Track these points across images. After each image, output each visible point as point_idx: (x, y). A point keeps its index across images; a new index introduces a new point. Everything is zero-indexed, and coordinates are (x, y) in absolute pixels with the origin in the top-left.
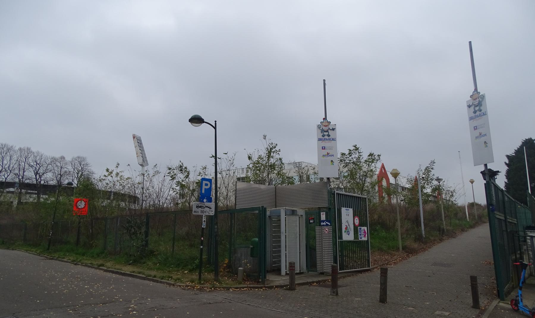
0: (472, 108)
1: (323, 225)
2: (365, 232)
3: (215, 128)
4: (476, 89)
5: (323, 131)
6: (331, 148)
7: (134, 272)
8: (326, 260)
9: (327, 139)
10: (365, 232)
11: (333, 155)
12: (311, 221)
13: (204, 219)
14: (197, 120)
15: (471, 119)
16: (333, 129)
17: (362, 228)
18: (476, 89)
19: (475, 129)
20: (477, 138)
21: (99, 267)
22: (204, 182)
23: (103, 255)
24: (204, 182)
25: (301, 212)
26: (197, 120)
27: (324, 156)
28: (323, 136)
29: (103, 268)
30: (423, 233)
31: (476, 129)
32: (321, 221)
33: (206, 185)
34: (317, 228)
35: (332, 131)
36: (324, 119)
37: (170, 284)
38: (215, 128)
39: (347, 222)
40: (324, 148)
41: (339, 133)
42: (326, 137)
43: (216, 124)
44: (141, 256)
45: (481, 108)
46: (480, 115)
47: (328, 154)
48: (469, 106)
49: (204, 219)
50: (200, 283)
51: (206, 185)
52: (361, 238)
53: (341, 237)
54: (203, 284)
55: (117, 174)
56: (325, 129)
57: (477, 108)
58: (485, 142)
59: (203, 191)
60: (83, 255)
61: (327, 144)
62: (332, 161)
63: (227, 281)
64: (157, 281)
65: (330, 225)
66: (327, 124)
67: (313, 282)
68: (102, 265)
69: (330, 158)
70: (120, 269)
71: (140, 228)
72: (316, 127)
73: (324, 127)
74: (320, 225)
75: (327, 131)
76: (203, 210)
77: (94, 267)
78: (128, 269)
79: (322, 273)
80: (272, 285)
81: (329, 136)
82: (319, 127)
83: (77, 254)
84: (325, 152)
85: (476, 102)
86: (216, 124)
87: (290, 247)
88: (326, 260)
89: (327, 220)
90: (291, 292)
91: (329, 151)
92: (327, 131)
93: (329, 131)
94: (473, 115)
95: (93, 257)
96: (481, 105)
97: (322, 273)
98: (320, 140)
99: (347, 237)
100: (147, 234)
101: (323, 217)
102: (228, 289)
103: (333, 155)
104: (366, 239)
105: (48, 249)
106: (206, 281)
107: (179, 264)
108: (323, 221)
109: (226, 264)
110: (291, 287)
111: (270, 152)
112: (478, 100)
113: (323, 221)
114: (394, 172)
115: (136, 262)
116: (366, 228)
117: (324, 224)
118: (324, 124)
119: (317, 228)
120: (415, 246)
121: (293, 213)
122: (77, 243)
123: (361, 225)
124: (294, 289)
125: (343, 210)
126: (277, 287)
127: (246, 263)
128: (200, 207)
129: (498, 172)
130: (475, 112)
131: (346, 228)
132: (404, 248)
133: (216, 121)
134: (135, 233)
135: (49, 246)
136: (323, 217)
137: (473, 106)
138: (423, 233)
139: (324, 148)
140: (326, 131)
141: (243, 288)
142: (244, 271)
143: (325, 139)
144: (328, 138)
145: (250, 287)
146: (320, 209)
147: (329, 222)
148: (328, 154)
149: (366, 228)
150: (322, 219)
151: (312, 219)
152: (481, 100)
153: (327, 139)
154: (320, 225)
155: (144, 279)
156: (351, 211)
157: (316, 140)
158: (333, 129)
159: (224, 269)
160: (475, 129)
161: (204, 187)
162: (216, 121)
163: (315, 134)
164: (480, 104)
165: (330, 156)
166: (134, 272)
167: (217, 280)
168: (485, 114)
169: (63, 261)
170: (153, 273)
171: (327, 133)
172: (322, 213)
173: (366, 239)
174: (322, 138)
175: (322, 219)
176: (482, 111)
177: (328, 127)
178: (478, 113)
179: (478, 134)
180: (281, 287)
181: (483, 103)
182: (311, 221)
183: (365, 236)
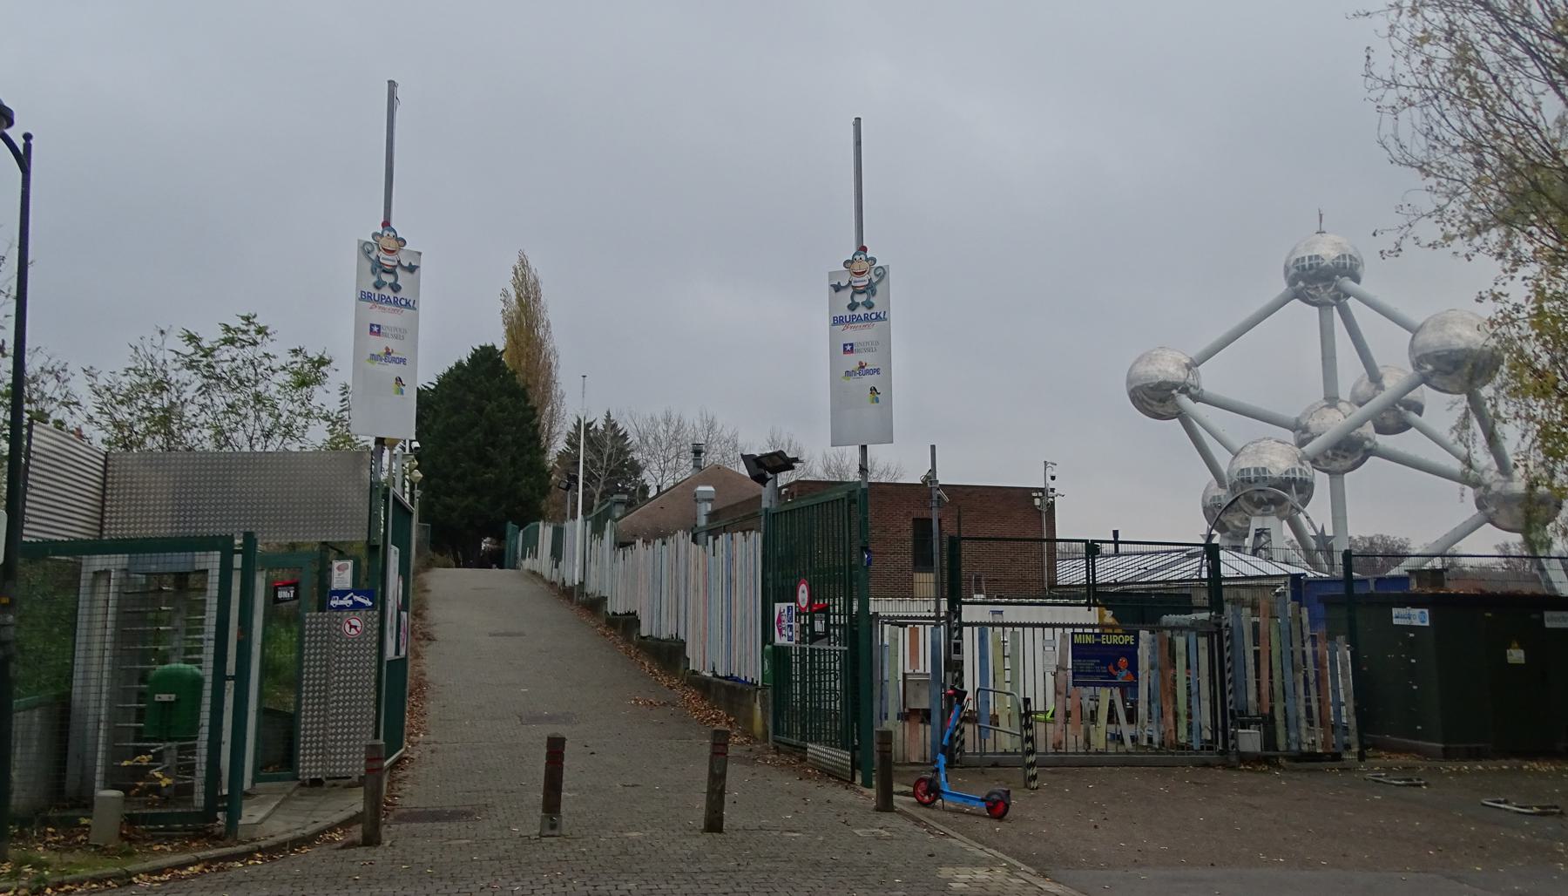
0: (845, 297)
5: (378, 267)
9: (388, 301)
11: (403, 361)
16: (412, 269)
27: (374, 357)
28: (378, 286)
31: (852, 351)
32: (325, 592)
34: (311, 616)
40: (376, 330)
41: (429, 287)
42: (387, 292)
45: (873, 300)
46: (867, 318)
56: (388, 261)
57: (860, 299)
58: (873, 390)
61: (387, 317)
62: (399, 380)
65: (373, 608)
66: (392, 245)
69: (393, 370)
73: (382, 255)
74: (323, 606)
75: (392, 272)
81: (396, 288)
84: (377, 345)
85: (862, 282)
91: (392, 343)
93: (398, 270)
96: (874, 294)
101: (342, 576)
103: (403, 361)
112: (866, 277)
113: (342, 594)
117: (346, 602)
118: (384, 242)
119: (311, 616)
130: (853, 306)
136: (342, 576)
137: (850, 291)
139: (376, 330)
140: (388, 270)
143: (382, 297)
144: (392, 295)
146: (330, 551)
147: (369, 594)
148: (388, 353)
151: (286, 585)
152: (875, 280)
153: (388, 301)
154: (323, 606)
164: (870, 289)
165: (394, 360)
171: (389, 279)
172: (336, 564)
174: (373, 291)
176: (874, 310)
178: (861, 311)
179: (854, 366)
181: (879, 288)
182: (282, 594)
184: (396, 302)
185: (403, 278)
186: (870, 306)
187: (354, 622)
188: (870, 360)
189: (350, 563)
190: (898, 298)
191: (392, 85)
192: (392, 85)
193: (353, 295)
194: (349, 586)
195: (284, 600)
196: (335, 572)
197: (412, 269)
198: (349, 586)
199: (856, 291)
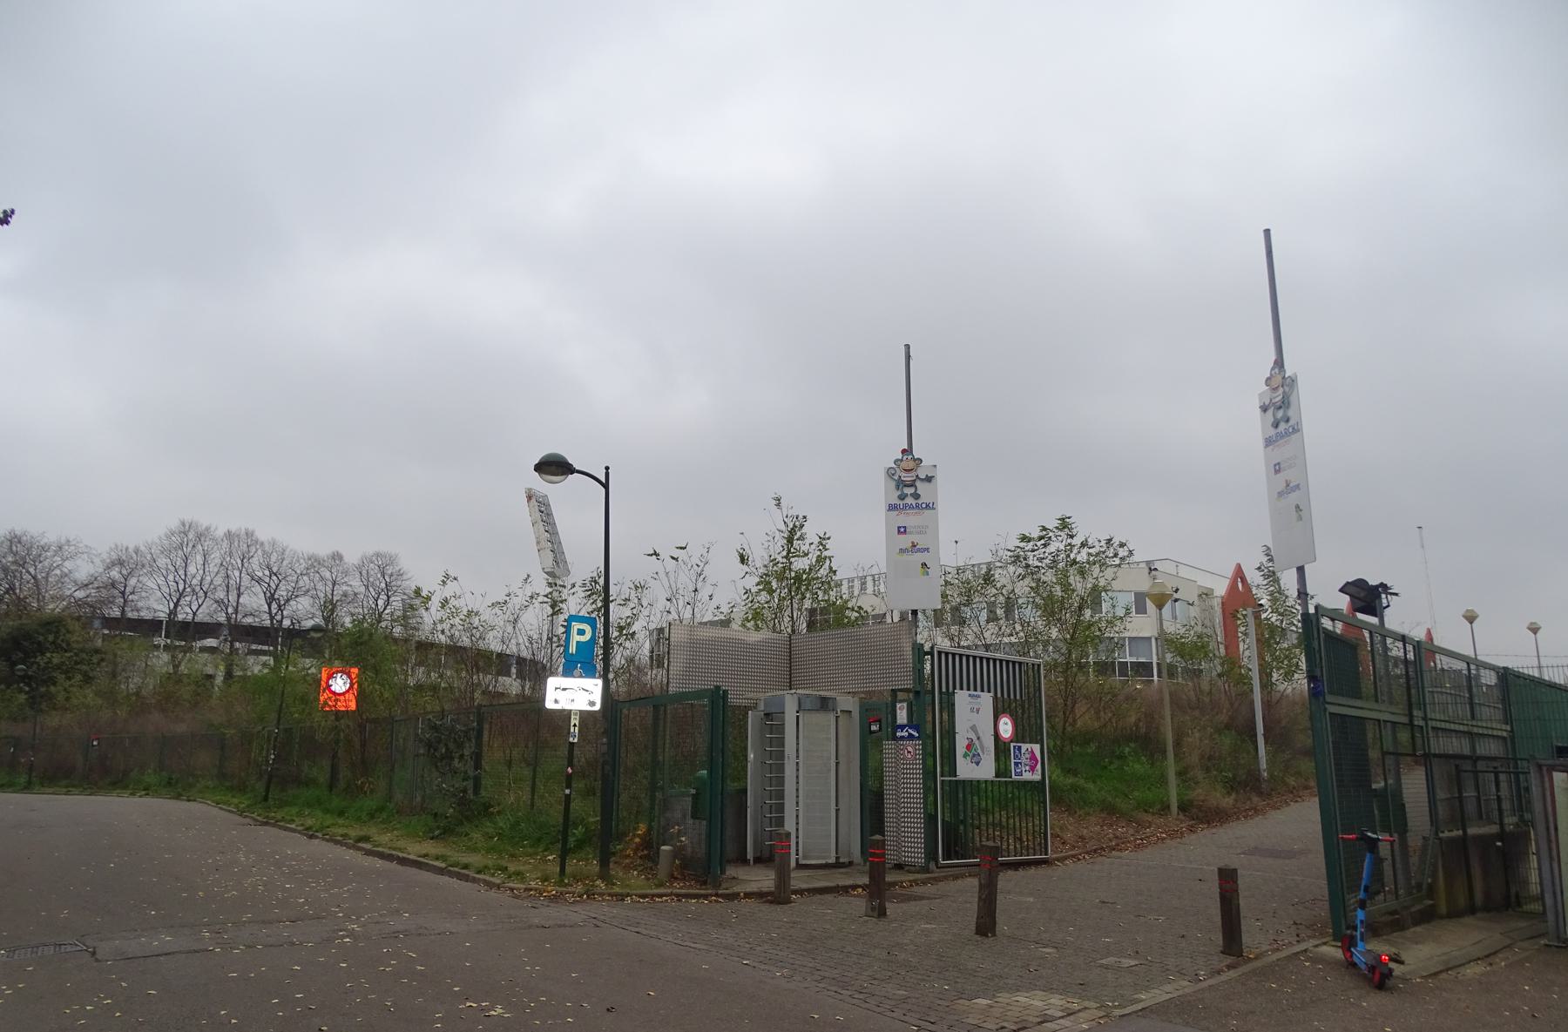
2: (1033, 757)
3: (606, 486)
4: (1279, 363)
5: (901, 484)
6: (922, 531)
7: (425, 856)
8: (907, 835)
9: (911, 507)
11: (927, 550)
12: (875, 724)
13: (575, 720)
15: (1269, 442)
16: (929, 479)
17: (1024, 747)
18: (1279, 363)
19: (1277, 472)
20: (1280, 494)
22: (576, 626)
23: (384, 815)
24: (576, 626)
25: (847, 703)
27: (902, 551)
28: (902, 497)
29: (368, 846)
30: (1263, 765)
34: (888, 745)
35: (926, 484)
36: (904, 451)
37: (490, 885)
38: (606, 486)
39: (974, 728)
40: (902, 531)
42: (910, 500)
44: (462, 814)
45: (1290, 413)
48: (1264, 409)
49: (575, 720)
50: (560, 883)
51: (581, 632)
54: (566, 885)
55: (444, 603)
56: (907, 477)
57: (1280, 414)
58: (1297, 507)
59: (573, 649)
60: (341, 814)
61: (911, 520)
62: (924, 565)
63: (636, 880)
64: (466, 878)
66: (911, 465)
67: (854, 887)
68: (366, 839)
69: (919, 558)
70: (400, 850)
71: (460, 746)
72: (882, 475)
75: (912, 484)
77: (345, 845)
78: (414, 849)
80: (736, 889)
81: (916, 496)
82: (890, 473)
83: (326, 811)
87: (811, 794)
89: (910, 725)
90: (779, 908)
92: (912, 484)
93: (918, 484)
94: (1272, 432)
95: (359, 819)
98: (892, 508)
99: (976, 769)
100: (477, 759)
101: (902, 716)
103: (927, 550)
104: (1037, 777)
105: (266, 799)
106: (577, 878)
107: (539, 840)
108: (902, 727)
110: (779, 896)
111: (790, 540)
113: (902, 727)
115: (445, 831)
117: (905, 734)
118: (904, 465)
119: (888, 745)
120: (1222, 799)
121: (825, 704)
123: (1020, 735)
124: (788, 901)
125: (962, 698)
126: (748, 895)
127: (689, 835)
129: (1341, 590)
130: (1276, 425)
131: (968, 747)
132: (1184, 808)
134: (449, 756)
135: (267, 791)
136: (902, 716)
138: (1263, 765)
139: (902, 531)
140: (909, 483)
141: (660, 896)
142: (678, 853)
143: (905, 506)
145: (677, 895)
147: (917, 728)
149: (1036, 748)
150: (899, 721)
153: (911, 507)
154: (895, 738)
155: (441, 871)
156: (986, 700)
157: (883, 508)
158: (929, 479)
160: (1277, 472)
161: (576, 638)
163: (880, 492)
164: (1285, 404)
165: (919, 550)
166: (425, 856)
167: (604, 875)
168: (1296, 430)
169: (286, 829)
170: (475, 859)
175: (899, 721)
177: (913, 473)
178: (1283, 426)
179: (1282, 486)
180: (760, 895)
181: (1293, 399)
182: (874, 728)
183: (1033, 769)
190: (1309, 407)
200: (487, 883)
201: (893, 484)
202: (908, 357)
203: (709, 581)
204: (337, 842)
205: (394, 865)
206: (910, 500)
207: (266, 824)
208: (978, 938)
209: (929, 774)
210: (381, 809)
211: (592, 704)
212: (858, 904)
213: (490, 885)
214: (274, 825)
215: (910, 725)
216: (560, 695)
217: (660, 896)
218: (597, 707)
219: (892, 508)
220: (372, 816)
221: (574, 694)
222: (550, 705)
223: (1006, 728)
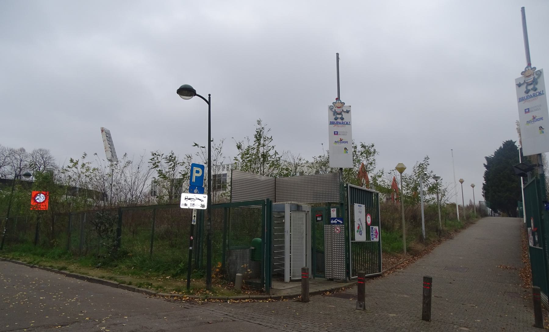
0: (523, 88)
1: (334, 224)
2: (376, 232)
3: (209, 103)
4: (529, 64)
5: (335, 113)
6: (345, 134)
7: (103, 277)
8: (336, 265)
9: (340, 123)
10: (376, 232)
12: (319, 217)
13: (194, 214)
14: (186, 91)
15: (521, 100)
16: (348, 112)
17: (374, 227)
18: (529, 64)
20: (528, 122)
21: (60, 270)
22: (195, 169)
23: (66, 256)
24: (195, 169)
25: (306, 207)
26: (186, 91)
29: (65, 272)
30: (424, 234)
32: (330, 219)
33: (197, 172)
34: (327, 227)
35: (346, 114)
36: (337, 99)
37: (150, 294)
38: (209, 103)
39: (360, 220)
40: (336, 133)
42: (339, 120)
43: (210, 98)
44: (113, 257)
45: (537, 86)
46: (535, 95)
47: (341, 140)
48: (519, 85)
49: (194, 214)
50: (188, 293)
52: (373, 239)
53: (353, 239)
54: (192, 294)
56: (338, 110)
57: (530, 87)
59: (194, 180)
60: (42, 255)
61: (339, 129)
62: (346, 149)
63: (223, 290)
64: (134, 290)
66: (340, 105)
67: (326, 291)
68: (65, 268)
69: (344, 145)
70: (86, 274)
71: (111, 225)
73: (336, 109)
76: (193, 202)
77: (54, 271)
78: (95, 273)
79: (331, 280)
81: (342, 119)
82: (331, 108)
83: (34, 254)
84: (337, 138)
85: (531, 79)
86: (210, 98)
88: (336, 265)
89: (338, 218)
90: (306, 304)
91: (342, 137)
93: (343, 113)
94: (525, 95)
95: (53, 258)
96: (537, 83)
97: (331, 280)
98: (331, 123)
99: (360, 237)
100: (119, 232)
101: (334, 214)
102: (225, 300)
106: (197, 290)
107: (159, 268)
108: (334, 219)
109: (218, 268)
110: (304, 298)
112: (532, 77)
113: (334, 219)
114: (400, 167)
115: (105, 265)
116: (377, 228)
117: (335, 222)
118: (337, 105)
119: (327, 227)
120: (420, 247)
121: (298, 208)
122: (36, 242)
123: (374, 223)
124: (308, 301)
126: (285, 297)
127: (242, 268)
128: (189, 199)
130: (527, 92)
131: (359, 228)
132: (409, 250)
133: (210, 95)
134: (106, 230)
136: (334, 214)
137: (525, 85)
138: (424, 234)
139: (336, 133)
141: (244, 299)
142: (243, 277)
143: (337, 122)
144: (341, 121)
145: (253, 299)
146: (329, 205)
148: (341, 140)
149: (377, 228)
150: (332, 216)
152: (536, 77)
153: (340, 123)
154: (330, 223)
156: (363, 206)
159: (216, 275)
160: (526, 112)
161: (195, 175)
162: (210, 95)
163: (325, 116)
164: (535, 82)
165: (343, 142)
166: (103, 277)
168: (542, 93)
169: (16, 263)
170: (127, 279)
171: (339, 116)
172: (332, 209)
173: (378, 240)
174: (334, 121)
175: (332, 216)
176: (537, 91)
177: (341, 109)
178: (531, 93)
179: (531, 118)
180: (290, 297)
181: (539, 80)
182: (318, 219)
184: (343, 123)
185: (345, 115)
186: (535, 89)
187: (338, 228)
188: (538, 115)
189: (335, 209)
191: (338, 54)
192: (338, 54)
193: (327, 122)
194: (335, 216)
195: (319, 221)
196: (332, 212)
197: (348, 112)
198: (335, 216)
199: (529, 84)
200: (147, 293)
201: (332, 113)
202: (338, 59)
203: (223, 155)
204: (48, 270)
205: (86, 283)
206: (339, 120)
207: (5, 260)
208: (424, 322)
209: (347, 239)
210: (64, 253)
211: (203, 206)
212: (352, 303)
213: (150, 294)
214: (9, 261)
215: (338, 218)
216: (189, 202)
217: (244, 299)
218: (205, 208)
219: (331, 123)
220: (60, 257)
221: (194, 202)
222: (182, 206)
223: (369, 220)
